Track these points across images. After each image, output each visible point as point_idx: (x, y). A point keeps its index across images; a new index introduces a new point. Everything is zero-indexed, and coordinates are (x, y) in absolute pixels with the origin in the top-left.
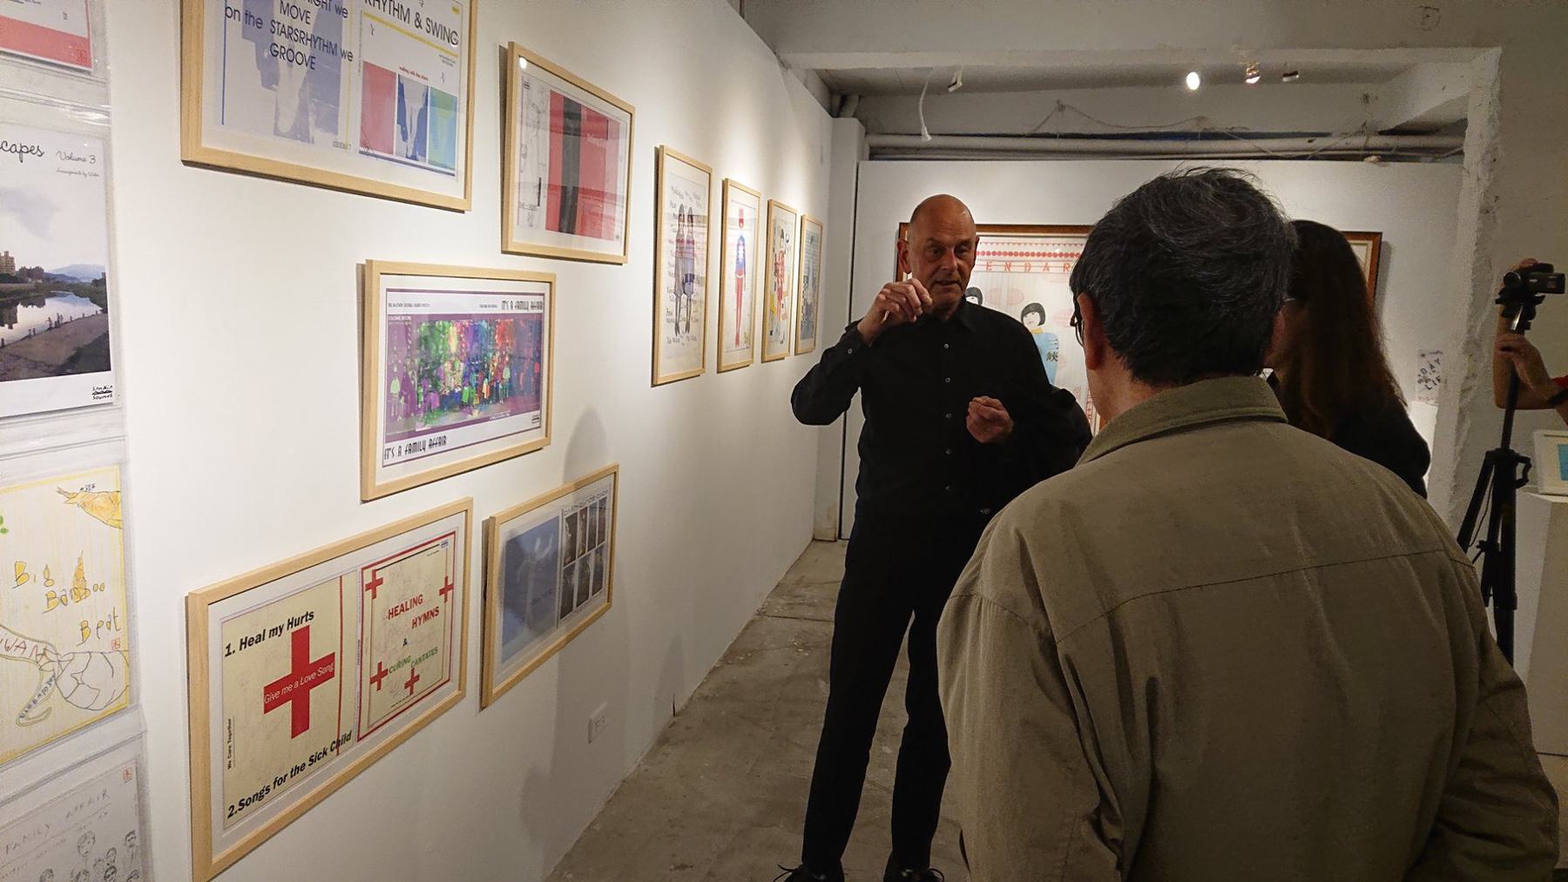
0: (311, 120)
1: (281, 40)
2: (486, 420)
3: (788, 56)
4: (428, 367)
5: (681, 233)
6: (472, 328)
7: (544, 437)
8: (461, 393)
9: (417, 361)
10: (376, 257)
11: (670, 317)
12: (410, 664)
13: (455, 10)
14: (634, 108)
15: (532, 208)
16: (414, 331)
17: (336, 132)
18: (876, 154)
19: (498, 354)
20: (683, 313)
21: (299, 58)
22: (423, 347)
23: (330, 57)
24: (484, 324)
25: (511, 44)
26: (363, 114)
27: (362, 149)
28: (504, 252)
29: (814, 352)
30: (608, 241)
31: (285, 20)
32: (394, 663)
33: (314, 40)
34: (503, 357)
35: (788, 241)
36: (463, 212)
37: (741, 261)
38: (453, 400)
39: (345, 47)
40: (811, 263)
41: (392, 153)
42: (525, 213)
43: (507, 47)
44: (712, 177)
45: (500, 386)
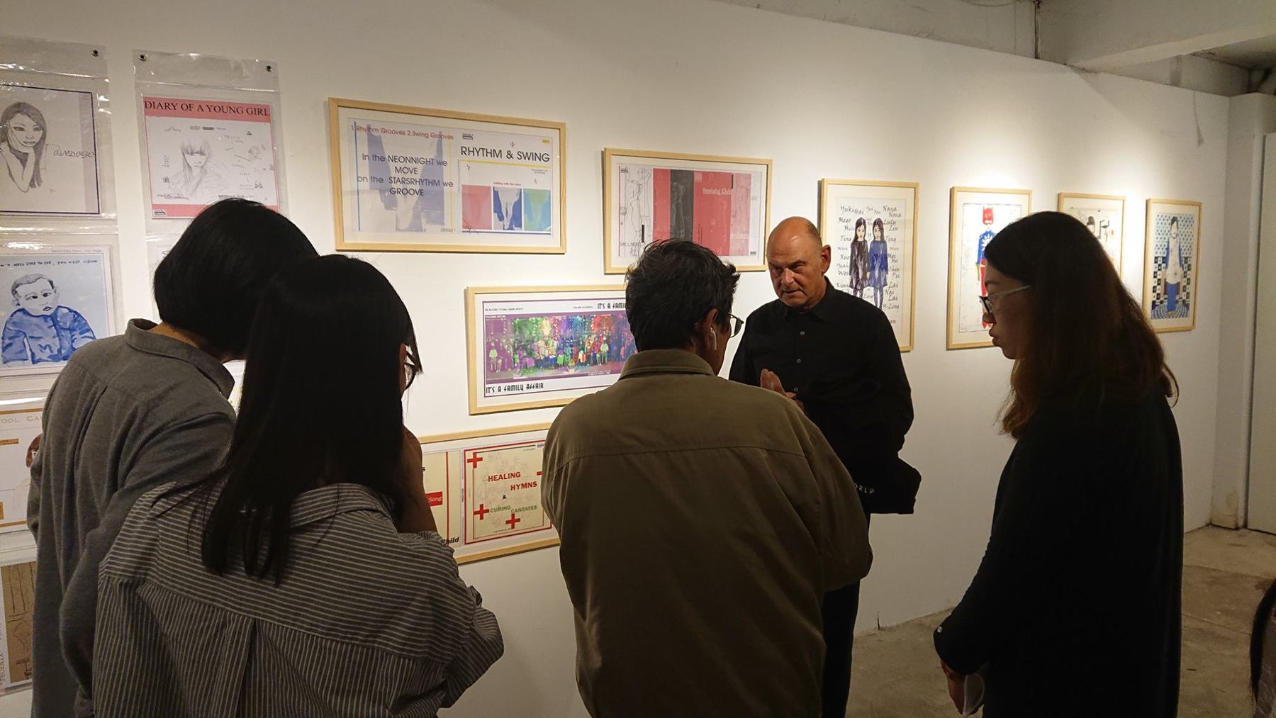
0: (423, 221)
1: (396, 186)
2: (587, 375)
4: (523, 343)
5: (860, 240)
6: (569, 321)
8: (556, 359)
9: (511, 340)
10: (472, 284)
12: (510, 510)
13: (544, 141)
14: (771, 161)
16: (509, 324)
17: (443, 224)
21: (412, 192)
22: (517, 333)
23: (436, 188)
25: (605, 149)
26: (464, 213)
27: (465, 230)
28: (605, 274)
29: (1193, 330)
30: (742, 257)
31: (400, 175)
32: (494, 506)
33: (421, 181)
36: (564, 254)
38: (548, 363)
39: (446, 180)
41: (491, 229)
43: (603, 150)
44: (920, 190)
45: (598, 355)
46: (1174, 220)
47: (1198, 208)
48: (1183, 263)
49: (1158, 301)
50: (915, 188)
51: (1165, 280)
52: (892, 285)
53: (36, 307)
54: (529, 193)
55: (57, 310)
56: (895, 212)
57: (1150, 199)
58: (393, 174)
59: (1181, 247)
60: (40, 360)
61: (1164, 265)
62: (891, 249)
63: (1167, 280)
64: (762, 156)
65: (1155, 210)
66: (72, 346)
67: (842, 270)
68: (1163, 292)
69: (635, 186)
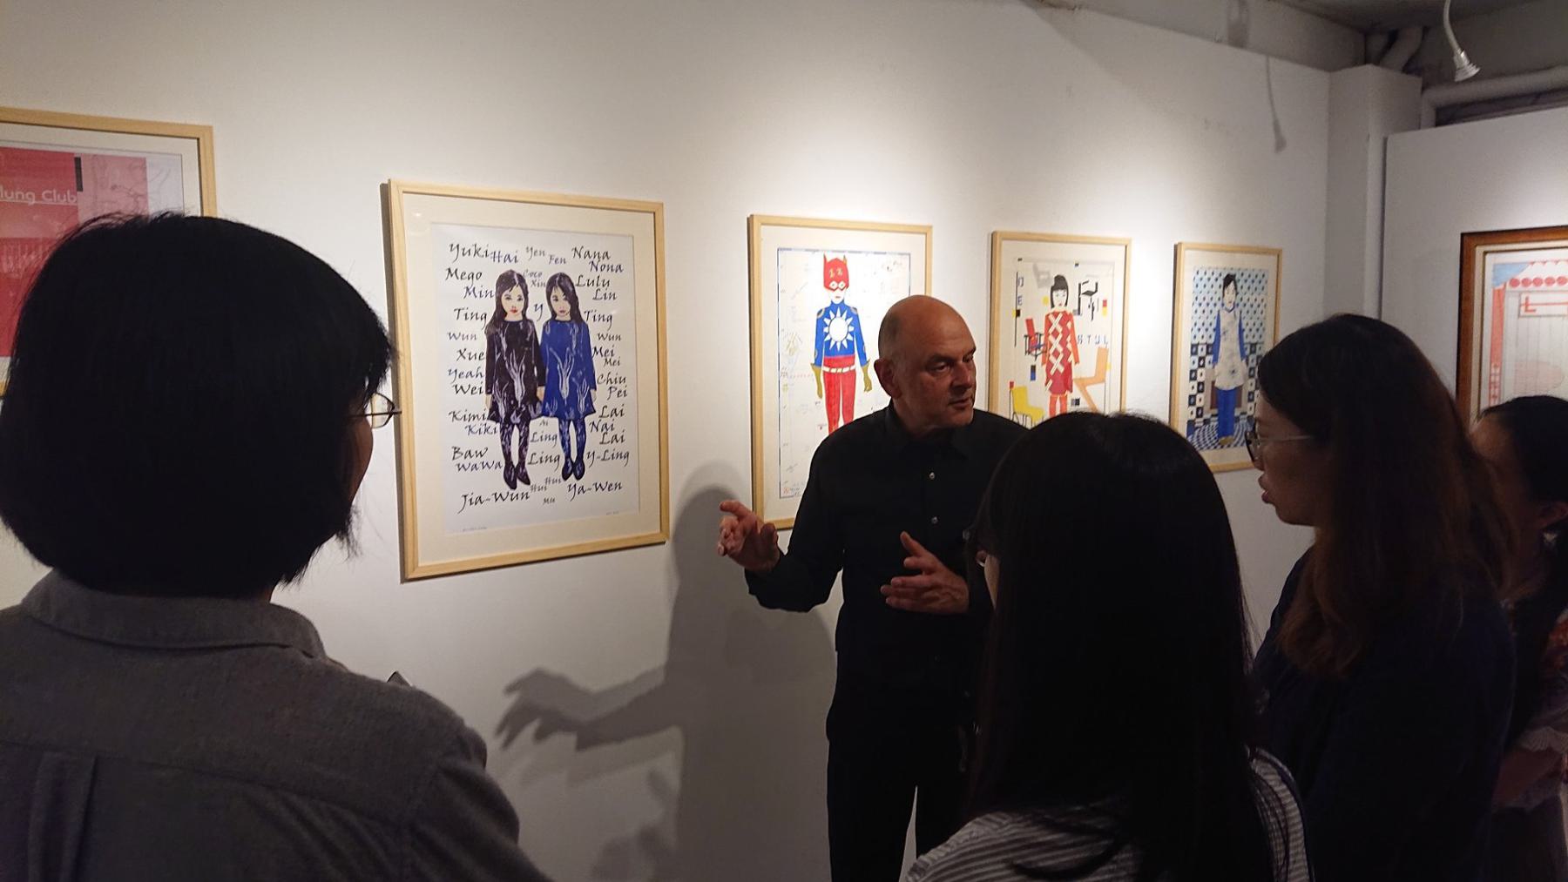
5: (510, 318)
18: (1447, 115)
44: (668, 217)
46: (1229, 279)
47: (1275, 258)
48: (1248, 352)
49: (1201, 420)
50: (654, 213)
51: (1213, 383)
52: (607, 412)
56: (605, 261)
57: (1180, 243)
59: (1244, 326)
61: (1209, 358)
62: (600, 337)
63: (1217, 384)
64: (195, 119)
65: (1189, 261)
67: (464, 382)
68: (1209, 407)
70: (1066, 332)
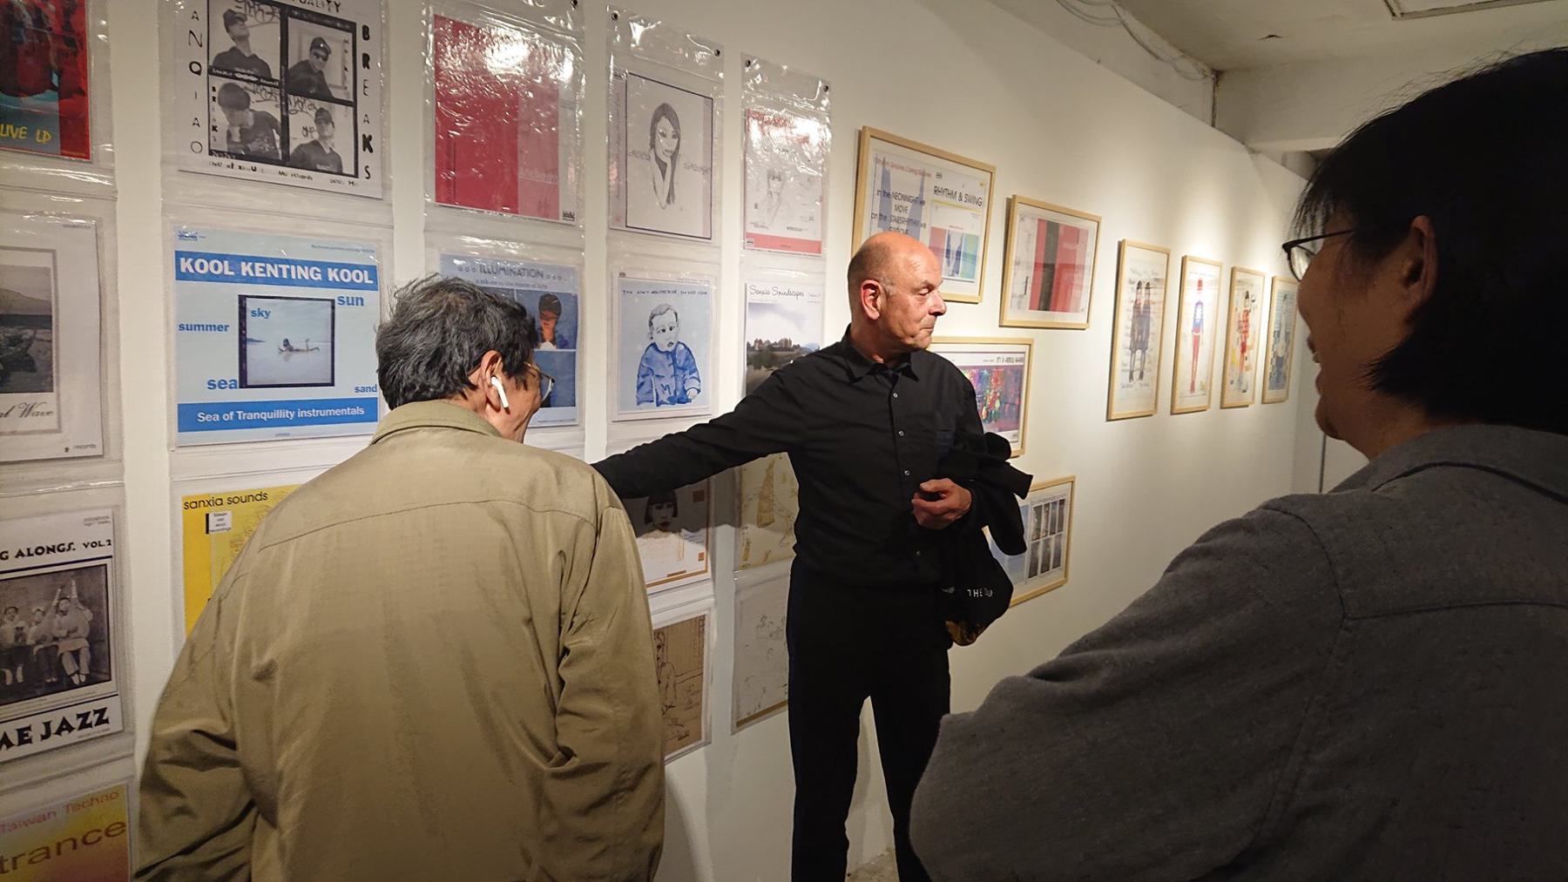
3: (1257, 145)
7: (1020, 448)
11: (1125, 368)
13: (981, 185)
14: (1100, 218)
15: (1021, 296)
19: (993, 391)
20: (1138, 364)
24: (985, 372)
25: (1014, 196)
28: (1000, 326)
29: (1287, 401)
34: (995, 393)
35: (1253, 301)
37: (1198, 321)
40: (1283, 318)
42: (1016, 300)
43: (1011, 197)
53: (663, 342)
54: (968, 235)
55: (676, 346)
58: (895, 214)
60: (663, 403)
66: (683, 387)
69: (1026, 234)
70: (1247, 321)
